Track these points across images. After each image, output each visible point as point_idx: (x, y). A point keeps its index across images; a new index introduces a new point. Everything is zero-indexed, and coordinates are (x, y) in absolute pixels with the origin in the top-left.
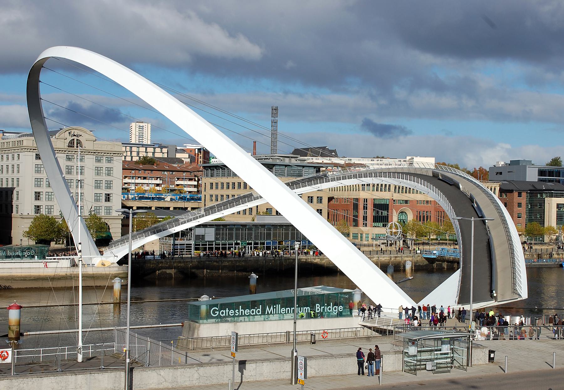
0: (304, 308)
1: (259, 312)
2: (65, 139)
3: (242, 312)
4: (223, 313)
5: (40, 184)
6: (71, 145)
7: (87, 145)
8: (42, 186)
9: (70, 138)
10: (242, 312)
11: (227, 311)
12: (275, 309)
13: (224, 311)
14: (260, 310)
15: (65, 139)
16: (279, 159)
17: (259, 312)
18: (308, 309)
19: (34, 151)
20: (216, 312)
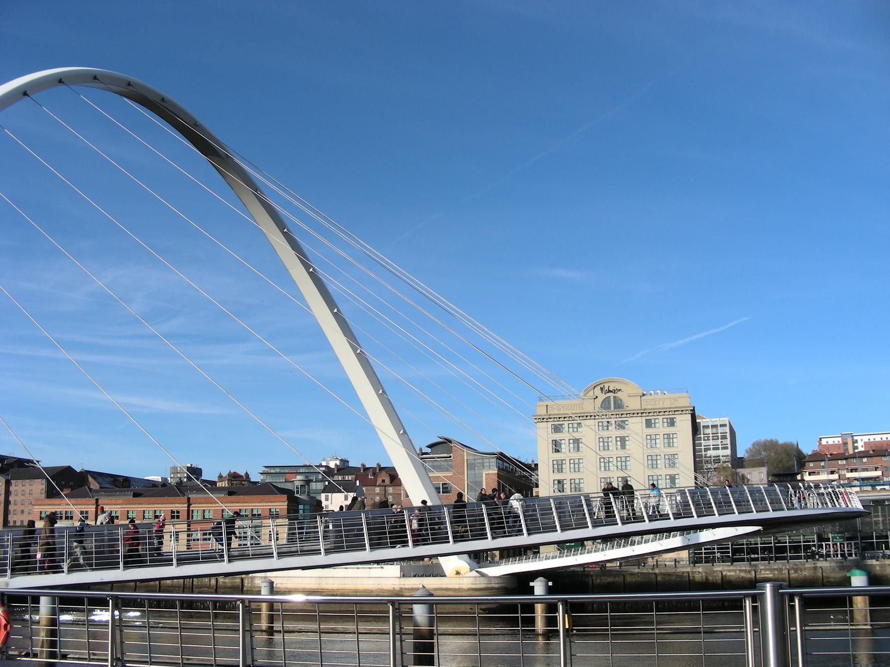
2: (595, 398)
5: (562, 469)
6: (605, 404)
7: (632, 404)
8: (564, 470)
9: (601, 397)
15: (595, 398)
19: (549, 420)
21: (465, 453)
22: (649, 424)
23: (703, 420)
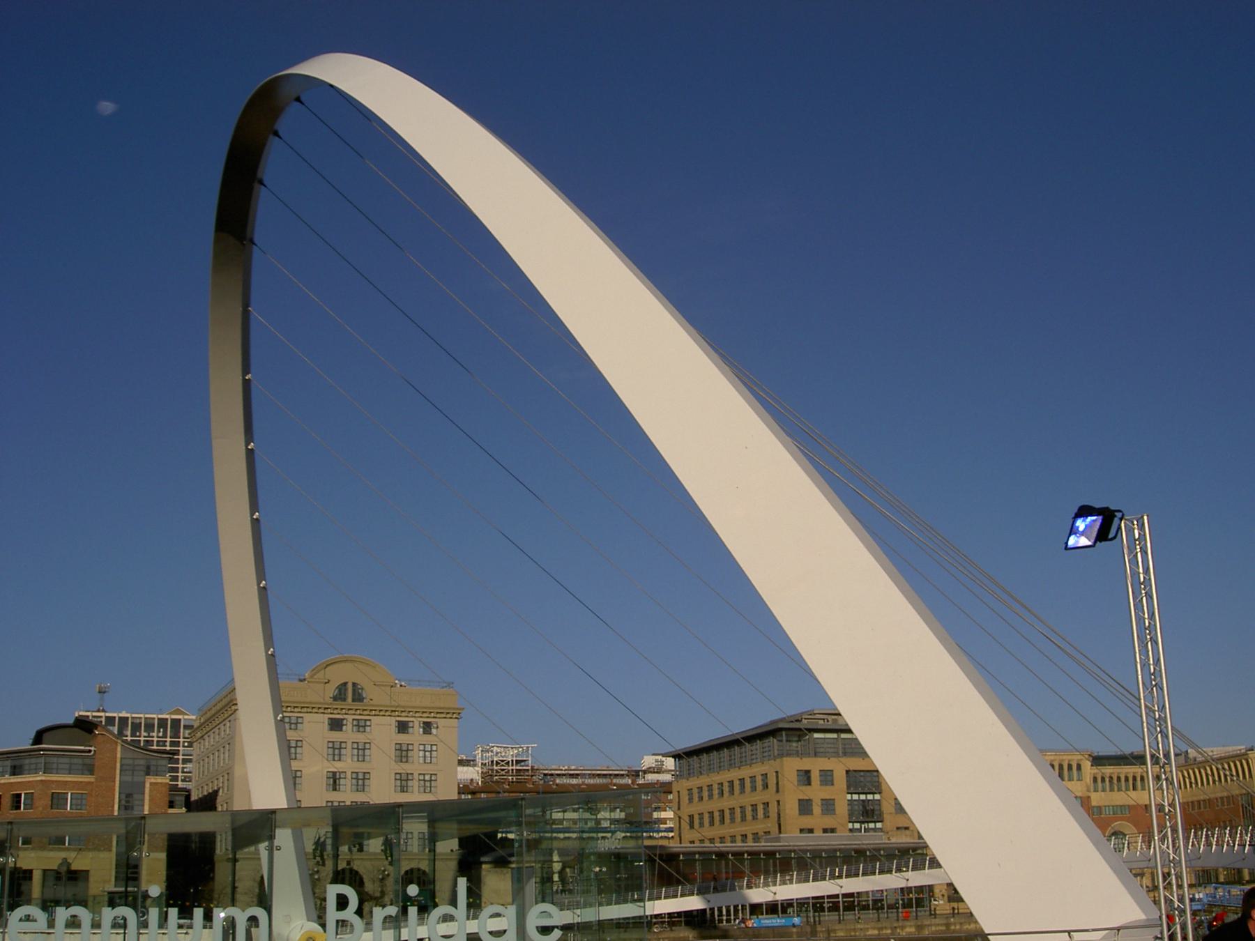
2: (326, 683)
15: (326, 683)
16: (824, 719)
21: (119, 748)
22: (403, 727)
23: (186, 717)
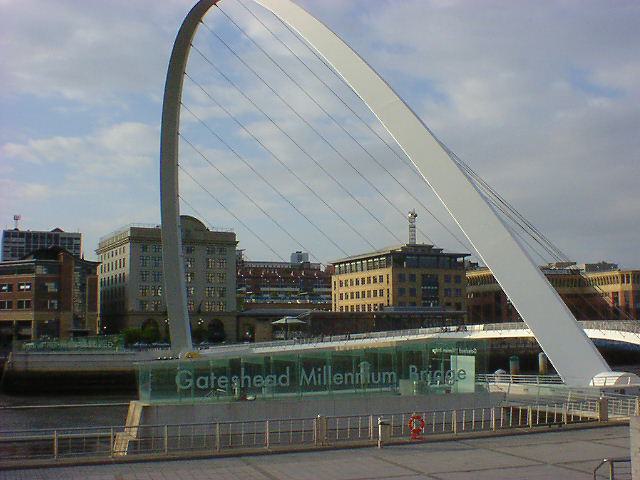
0: (384, 374)
1: (284, 380)
3: (246, 380)
4: (202, 382)
10: (246, 380)
11: (213, 378)
12: (319, 375)
13: (206, 379)
14: (288, 377)
17: (284, 380)
18: (392, 376)
20: (187, 381)
